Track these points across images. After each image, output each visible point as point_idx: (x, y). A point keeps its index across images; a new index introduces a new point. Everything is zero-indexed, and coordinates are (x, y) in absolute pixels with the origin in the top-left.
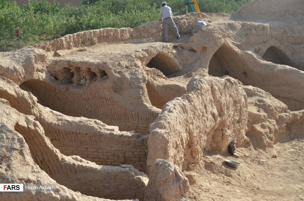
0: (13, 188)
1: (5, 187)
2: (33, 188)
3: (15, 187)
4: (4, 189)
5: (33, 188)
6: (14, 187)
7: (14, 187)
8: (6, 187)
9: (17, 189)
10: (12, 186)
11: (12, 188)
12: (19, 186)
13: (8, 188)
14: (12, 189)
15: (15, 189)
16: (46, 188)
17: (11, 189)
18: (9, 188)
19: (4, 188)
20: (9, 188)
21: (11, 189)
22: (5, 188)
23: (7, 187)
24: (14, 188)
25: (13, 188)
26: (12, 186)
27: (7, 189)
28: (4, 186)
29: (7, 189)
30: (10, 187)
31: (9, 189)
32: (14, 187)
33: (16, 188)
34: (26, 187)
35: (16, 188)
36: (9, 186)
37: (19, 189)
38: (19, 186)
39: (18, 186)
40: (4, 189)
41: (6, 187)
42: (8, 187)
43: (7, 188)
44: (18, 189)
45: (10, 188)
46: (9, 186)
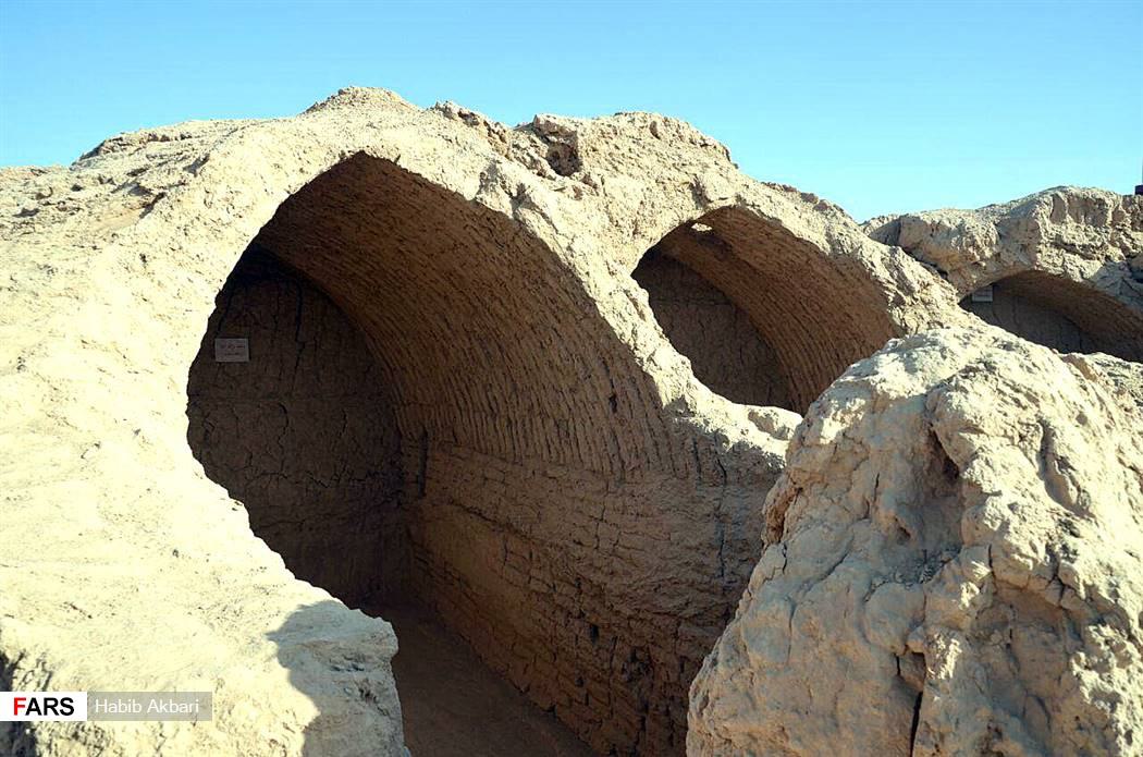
0: (49, 709)
1: (19, 703)
2: (123, 708)
3: (56, 704)
4: (16, 713)
5: (123, 708)
6: (52, 703)
7: (52, 703)
8: (23, 706)
9: (62, 712)
10: (46, 700)
11: (46, 707)
12: (71, 701)
13: (30, 709)
14: (46, 713)
15: (56, 713)
16: (174, 708)
17: (40, 714)
18: (34, 707)
19: (16, 706)
20: (34, 707)
21: (40, 714)
22: (19, 710)
23: (27, 703)
24: (52, 707)
25: (49, 709)
26: (46, 700)
27: (28, 713)
28: (16, 700)
29: (28, 713)
30: (37, 705)
31: (34, 710)
32: (51, 703)
33: (59, 707)
34: (97, 705)
35: (59, 707)
36: (34, 700)
37: (72, 710)
38: (71, 701)
39: (67, 702)
40: (16, 713)
41: (23, 706)
42: (31, 704)
43: (26, 709)
44: (67, 710)
45: (37, 709)
46: (34, 700)
